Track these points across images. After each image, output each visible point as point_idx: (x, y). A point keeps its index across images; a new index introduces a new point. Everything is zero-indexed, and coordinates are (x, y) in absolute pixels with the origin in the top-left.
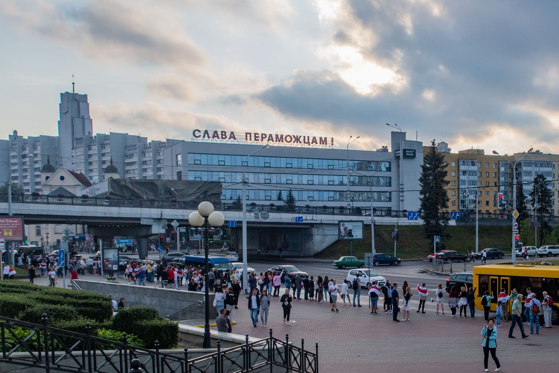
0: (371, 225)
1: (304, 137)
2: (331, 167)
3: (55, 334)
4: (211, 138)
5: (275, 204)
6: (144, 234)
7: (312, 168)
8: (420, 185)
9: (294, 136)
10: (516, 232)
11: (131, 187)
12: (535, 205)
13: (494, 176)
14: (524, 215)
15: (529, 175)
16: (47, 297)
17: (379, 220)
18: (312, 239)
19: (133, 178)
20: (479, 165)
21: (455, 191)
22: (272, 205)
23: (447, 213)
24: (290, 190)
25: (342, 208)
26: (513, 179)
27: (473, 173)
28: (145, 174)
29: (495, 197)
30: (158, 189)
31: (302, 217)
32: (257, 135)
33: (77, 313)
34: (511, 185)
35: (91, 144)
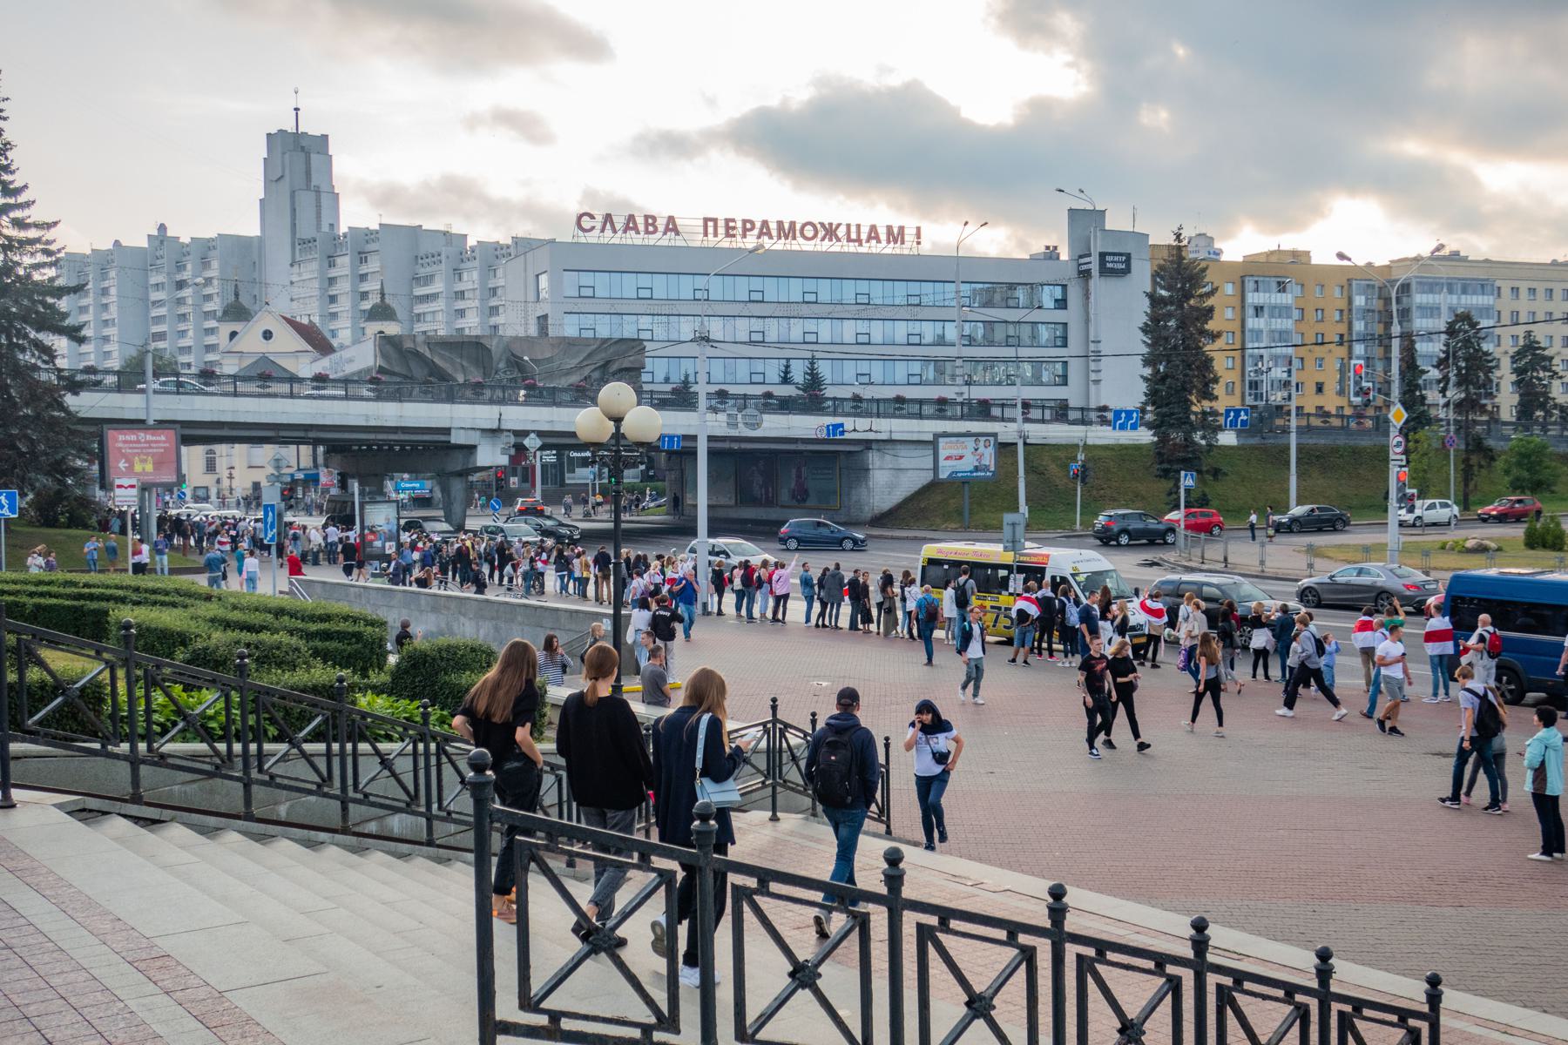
0: (1016, 444)
1: (848, 226)
2: (915, 301)
3: (259, 701)
4: (620, 232)
5: (775, 394)
6: (459, 468)
7: (869, 304)
8: (1144, 342)
9: (822, 225)
10: (1399, 463)
11: (428, 354)
12: (1449, 394)
13: (1337, 317)
14: (1419, 419)
15: (1432, 316)
16: (236, 616)
17: (1042, 433)
18: (866, 478)
19: (433, 333)
20: (1297, 290)
21: (1233, 358)
22: (768, 395)
23: (1215, 413)
24: (813, 358)
25: (942, 402)
26: (1388, 325)
27: (1282, 311)
28: (460, 323)
29: (1343, 371)
30: (491, 357)
31: (842, 425)
32: (731, 224)
33: (310, 652)
34: (1384, 340)
35: (336, 252)
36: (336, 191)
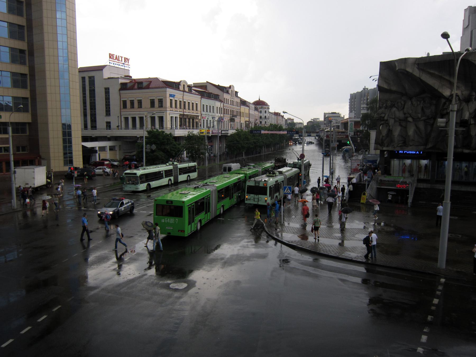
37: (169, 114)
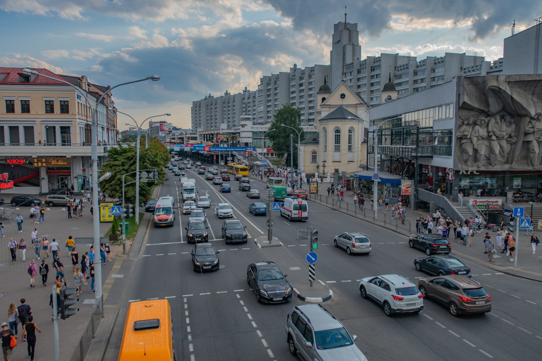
35: (361, 67)
36: (360, 45)
37: (78, 124)
